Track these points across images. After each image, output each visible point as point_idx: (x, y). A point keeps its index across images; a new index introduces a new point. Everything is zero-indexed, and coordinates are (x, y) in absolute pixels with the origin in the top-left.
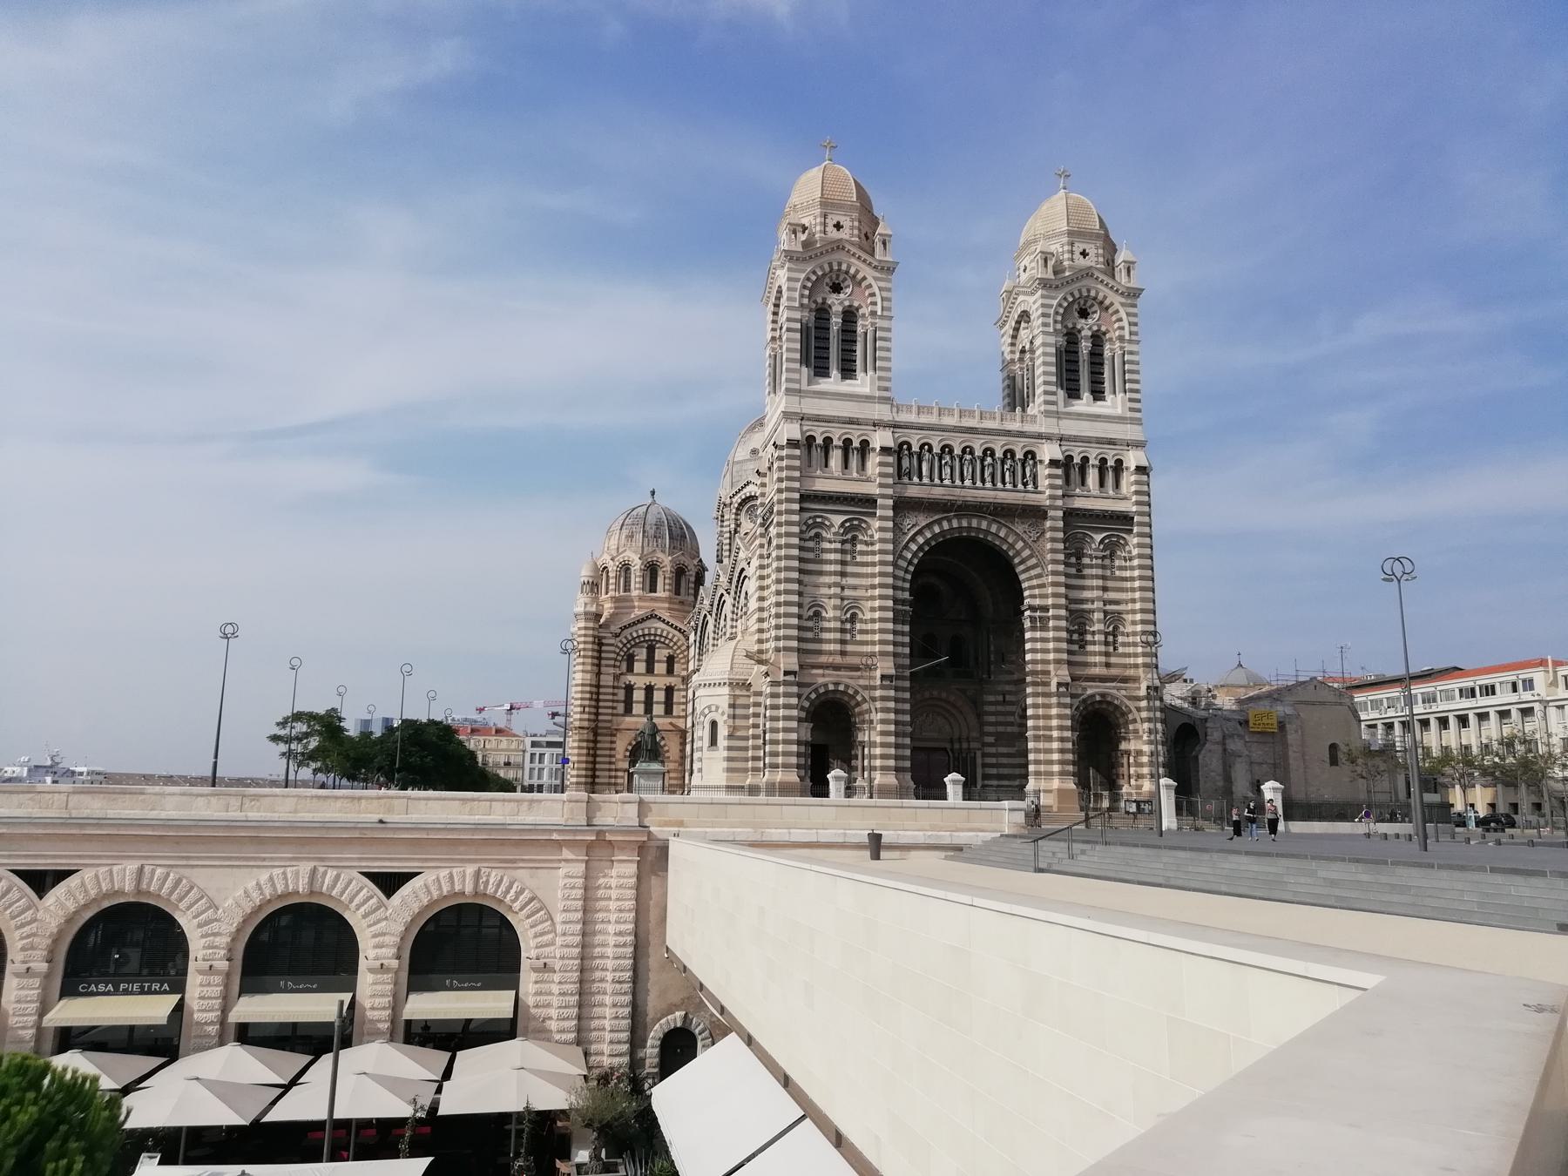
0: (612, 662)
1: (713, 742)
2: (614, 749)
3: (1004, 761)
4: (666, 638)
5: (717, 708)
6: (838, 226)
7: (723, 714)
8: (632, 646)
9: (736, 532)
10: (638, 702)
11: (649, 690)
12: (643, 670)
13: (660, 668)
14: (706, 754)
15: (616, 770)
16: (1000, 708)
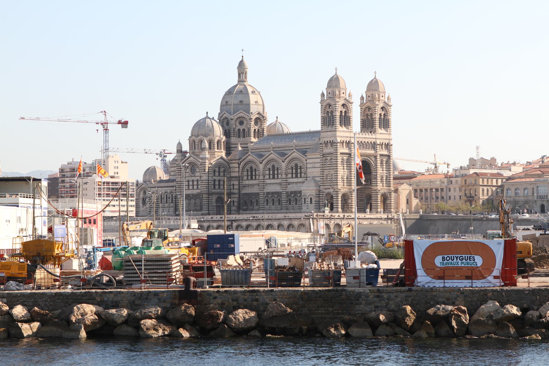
0: (211, 173)
1: (311, 202)
2: (212, 200)
3: (361, 205)
4: (225, 165)
5: (312, 195)
6: (343, 93)
7: (314, 196)
8: (215, 167)
9: (235, 128)
10: (217, 185)
11: (219, 181)
12: (218, 175)
13: (222, 174)
14: (309, 205)
15: (213, 206)
16: (361, 194)
